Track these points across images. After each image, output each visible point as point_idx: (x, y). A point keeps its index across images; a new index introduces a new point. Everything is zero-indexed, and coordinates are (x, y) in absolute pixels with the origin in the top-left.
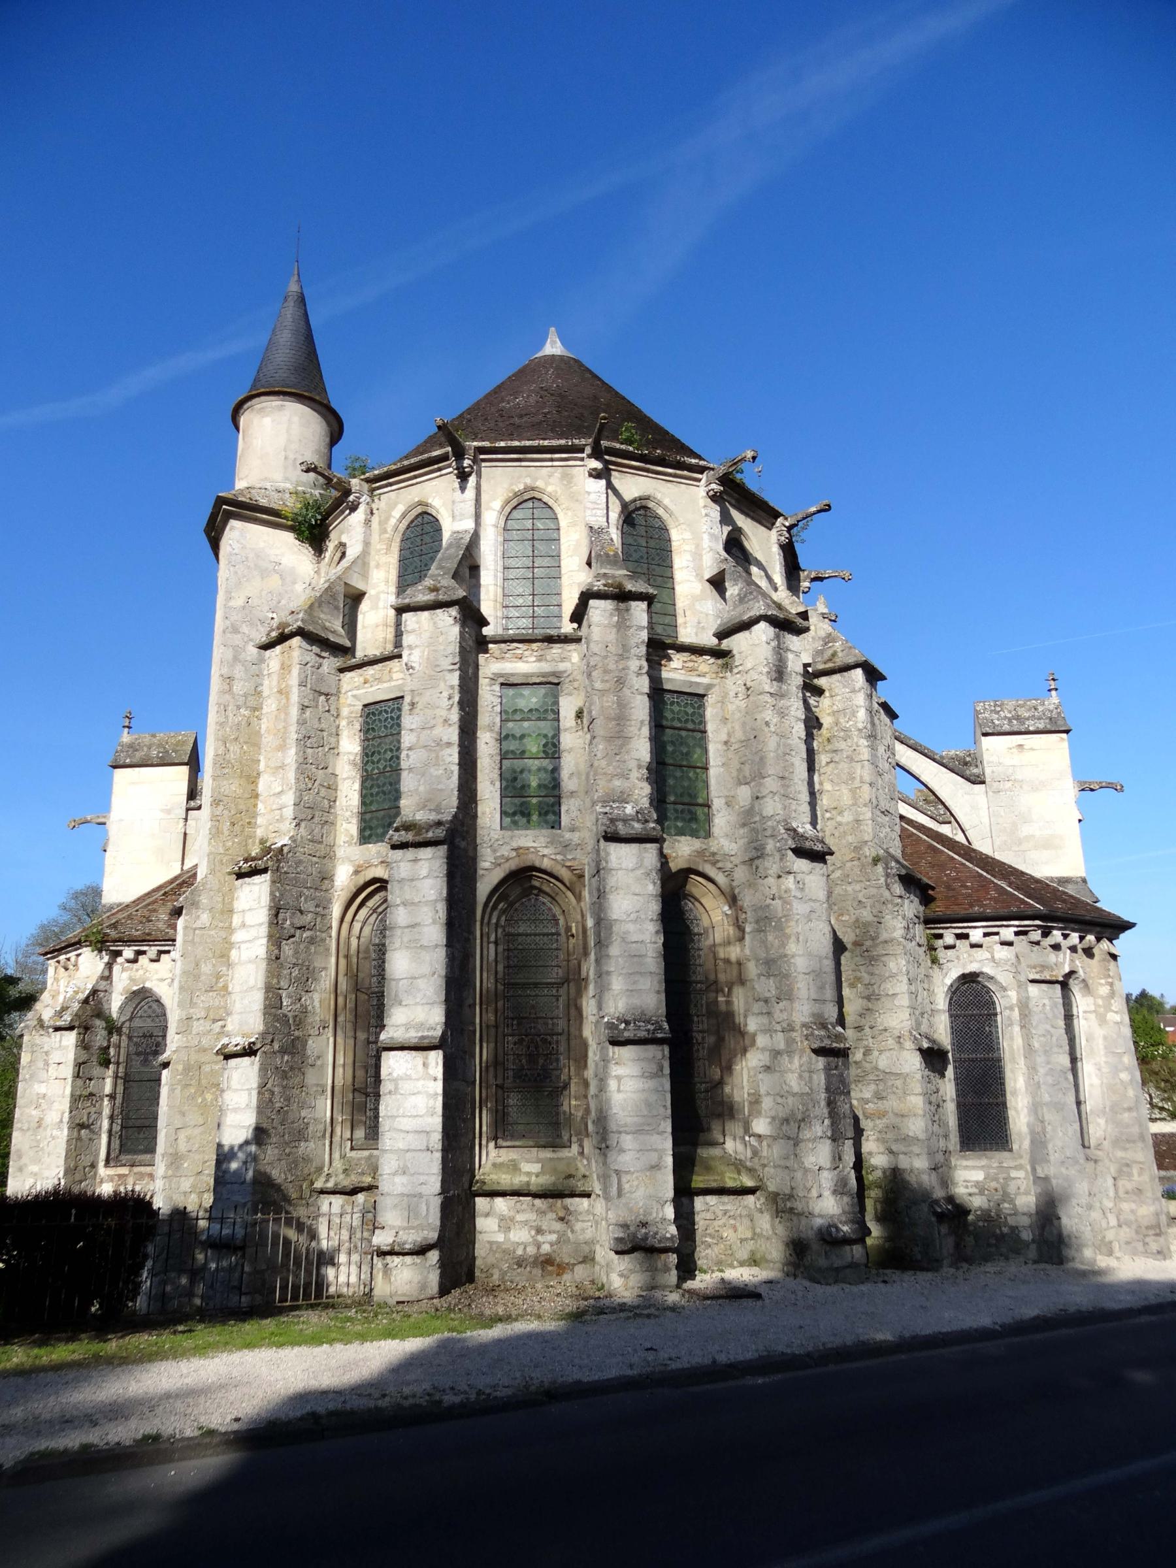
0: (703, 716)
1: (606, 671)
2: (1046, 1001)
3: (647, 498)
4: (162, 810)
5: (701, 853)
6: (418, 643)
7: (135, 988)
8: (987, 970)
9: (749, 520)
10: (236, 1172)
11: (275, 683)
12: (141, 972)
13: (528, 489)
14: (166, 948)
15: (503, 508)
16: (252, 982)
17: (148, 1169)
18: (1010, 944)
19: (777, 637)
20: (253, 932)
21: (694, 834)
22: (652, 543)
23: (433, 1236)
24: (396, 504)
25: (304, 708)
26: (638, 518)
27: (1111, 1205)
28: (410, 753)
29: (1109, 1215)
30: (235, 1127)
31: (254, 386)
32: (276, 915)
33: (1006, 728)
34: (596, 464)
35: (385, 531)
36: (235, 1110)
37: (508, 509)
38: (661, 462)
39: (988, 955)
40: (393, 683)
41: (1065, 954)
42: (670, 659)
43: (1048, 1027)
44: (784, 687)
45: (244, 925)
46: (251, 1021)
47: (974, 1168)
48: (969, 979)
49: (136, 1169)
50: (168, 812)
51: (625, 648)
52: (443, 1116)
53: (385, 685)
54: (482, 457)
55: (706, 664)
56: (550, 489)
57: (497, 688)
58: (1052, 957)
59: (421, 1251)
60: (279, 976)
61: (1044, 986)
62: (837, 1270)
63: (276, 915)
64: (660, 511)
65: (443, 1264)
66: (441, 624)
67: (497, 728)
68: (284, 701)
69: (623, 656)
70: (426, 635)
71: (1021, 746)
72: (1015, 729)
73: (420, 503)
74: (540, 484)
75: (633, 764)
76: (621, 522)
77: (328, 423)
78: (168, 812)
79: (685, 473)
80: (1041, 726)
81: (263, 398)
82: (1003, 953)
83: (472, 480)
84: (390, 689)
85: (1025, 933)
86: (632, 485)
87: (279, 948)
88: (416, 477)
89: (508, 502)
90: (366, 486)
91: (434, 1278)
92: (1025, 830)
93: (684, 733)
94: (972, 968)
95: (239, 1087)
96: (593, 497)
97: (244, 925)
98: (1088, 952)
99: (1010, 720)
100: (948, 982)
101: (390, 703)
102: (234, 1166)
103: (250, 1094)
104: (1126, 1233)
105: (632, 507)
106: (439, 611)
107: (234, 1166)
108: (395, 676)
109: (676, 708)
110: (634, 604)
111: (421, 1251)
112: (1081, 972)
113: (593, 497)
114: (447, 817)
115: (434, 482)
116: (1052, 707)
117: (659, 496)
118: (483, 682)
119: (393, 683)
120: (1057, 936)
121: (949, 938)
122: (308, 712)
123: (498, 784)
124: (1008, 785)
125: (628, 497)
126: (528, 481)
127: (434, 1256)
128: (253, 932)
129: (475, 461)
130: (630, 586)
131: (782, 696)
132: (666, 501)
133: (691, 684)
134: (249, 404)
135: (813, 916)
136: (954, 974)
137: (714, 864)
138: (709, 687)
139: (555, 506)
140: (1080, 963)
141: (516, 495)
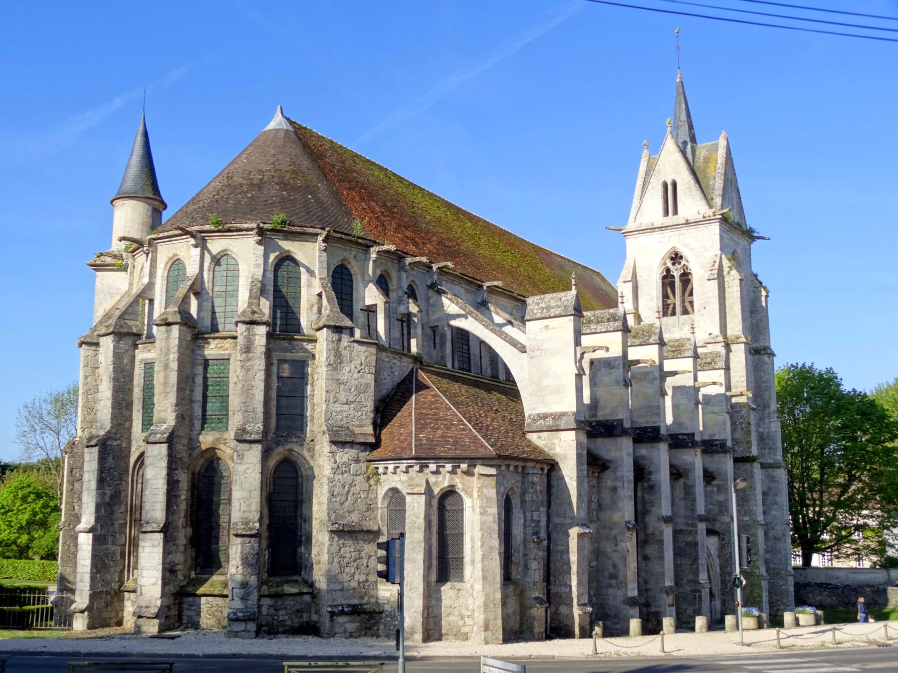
0: (228, 369)
1: (160, 362)
2: (415, 504)
3: (226, 250)
5: (218, 440)
8: (399, 486)
9: (296, 243)
13: (175, 255)
15: (165, 267)
18: (407, 472)
19: (248, 330)
21: (219, 430)
22: (230, 273)
23: (84, 606)
25: (86, 377)
26: (223, 261)
27: (469, 613)
29: (466, 619)
31: (118, 193)
32: (71, 472)
33: (539, 315)
34: (193, 241)
37: (168, 266)
38: (229, 230)
39: (398, 478)
41: (444, 476)
42: (209, 343)
43: (414, 518)
44: (251, 355)
47: (386, 590)
48: (394, 491)
51: (168, 349)
52: (92, 560)
55: (228, 343)
56: (182, 254)
57: (143, 366)
58: (432, 479)
59: (82, 612)
60: (73, 497)
61: (415, 496)
62: (236, 632)
63: (71, 472)
64: (234, 255)
65: (90, 617)
67: (142, 385)
69: (167, 354)
71: (547, 326)
72: (543, 316)
74: (178, 252)
75: (169, 405)
76: (212, 266)
77: (150, 205)
79: (245, 232)
80: (557, 313)
82: (404, 477)
83: (150, 255)
85: (412, 466)
86: (216, 245)
87: (73, 485)
89: (167, 263)
90: (130, 255)
91: (86, 621)
92: (546, 382)
93: (218, 380)
94: (393, 485)
96: (194, 258)
98: (469, 473)
99: (543, 308)
100: (383, 493)
104: (475, 628)
105: (219, 257)
109: (215, 367)
110: (173, 326)
111: (82, 612)
112: (460, 486)
113: (194, 258)
114: (102, 433)
116: (569, 298)
117: (231, 248)
118: (137, 363)
120: (433, 467)
121: (381, 470)
122: (89, 379)
123: (141, 412)
124: (538, 352)
125: (214, 252)
126: (174, 251)
127: (86, 613)
129: (150, 245)
130: (170, 320)
131: (249, 360)
132: (234, 250)
133: (220, 355)
135: (248, 471)
136: (386, 489)
137: (225, 444)
138: (230, 355)
140: (459, 481)
141: (170, 259)
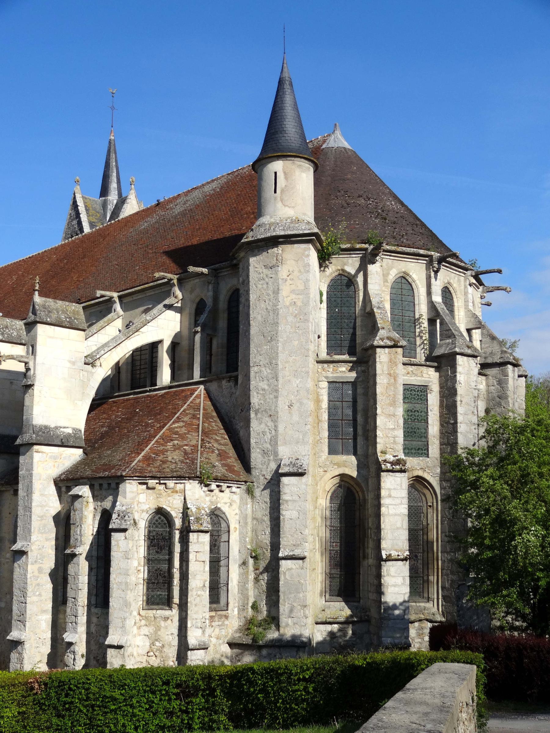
4: (70, 362)
6: (463, 372)
7: (213, 507)
10: (398, 615)
11: (385, 368)
12: (215, 498)
14: (231, 485)
16: (399, 525)
17: (224, 613)
20: (398, 501)
24: (392, 268)
28: (461, 425)
30: (395, 593)
35: (387, 281)
36: (395, 586)
40: (423, 379)
45: (390, 496)
46: (400, 544)
49: (219, 613)
50: (73, 363)
53: (419, 378)
54: (444, 263)
66: (471, 365)
68: (393, 380)
70: (466, 369)
73: (405, 273)
78: (73, 363)
81: (302, 160)
84: (421, 381)
88: (404, 258)
95: (397, 575)
97: (390, 496)
101: (417, 387)
102: (397, 612)
103: (404, 579)
106: (470, 358)
107: (397, 612)
108: (424, 375)
115: (413, 264)
119: (423, 379)
128: (398, 501)
134: (293, 159)
139: (454, 294)
